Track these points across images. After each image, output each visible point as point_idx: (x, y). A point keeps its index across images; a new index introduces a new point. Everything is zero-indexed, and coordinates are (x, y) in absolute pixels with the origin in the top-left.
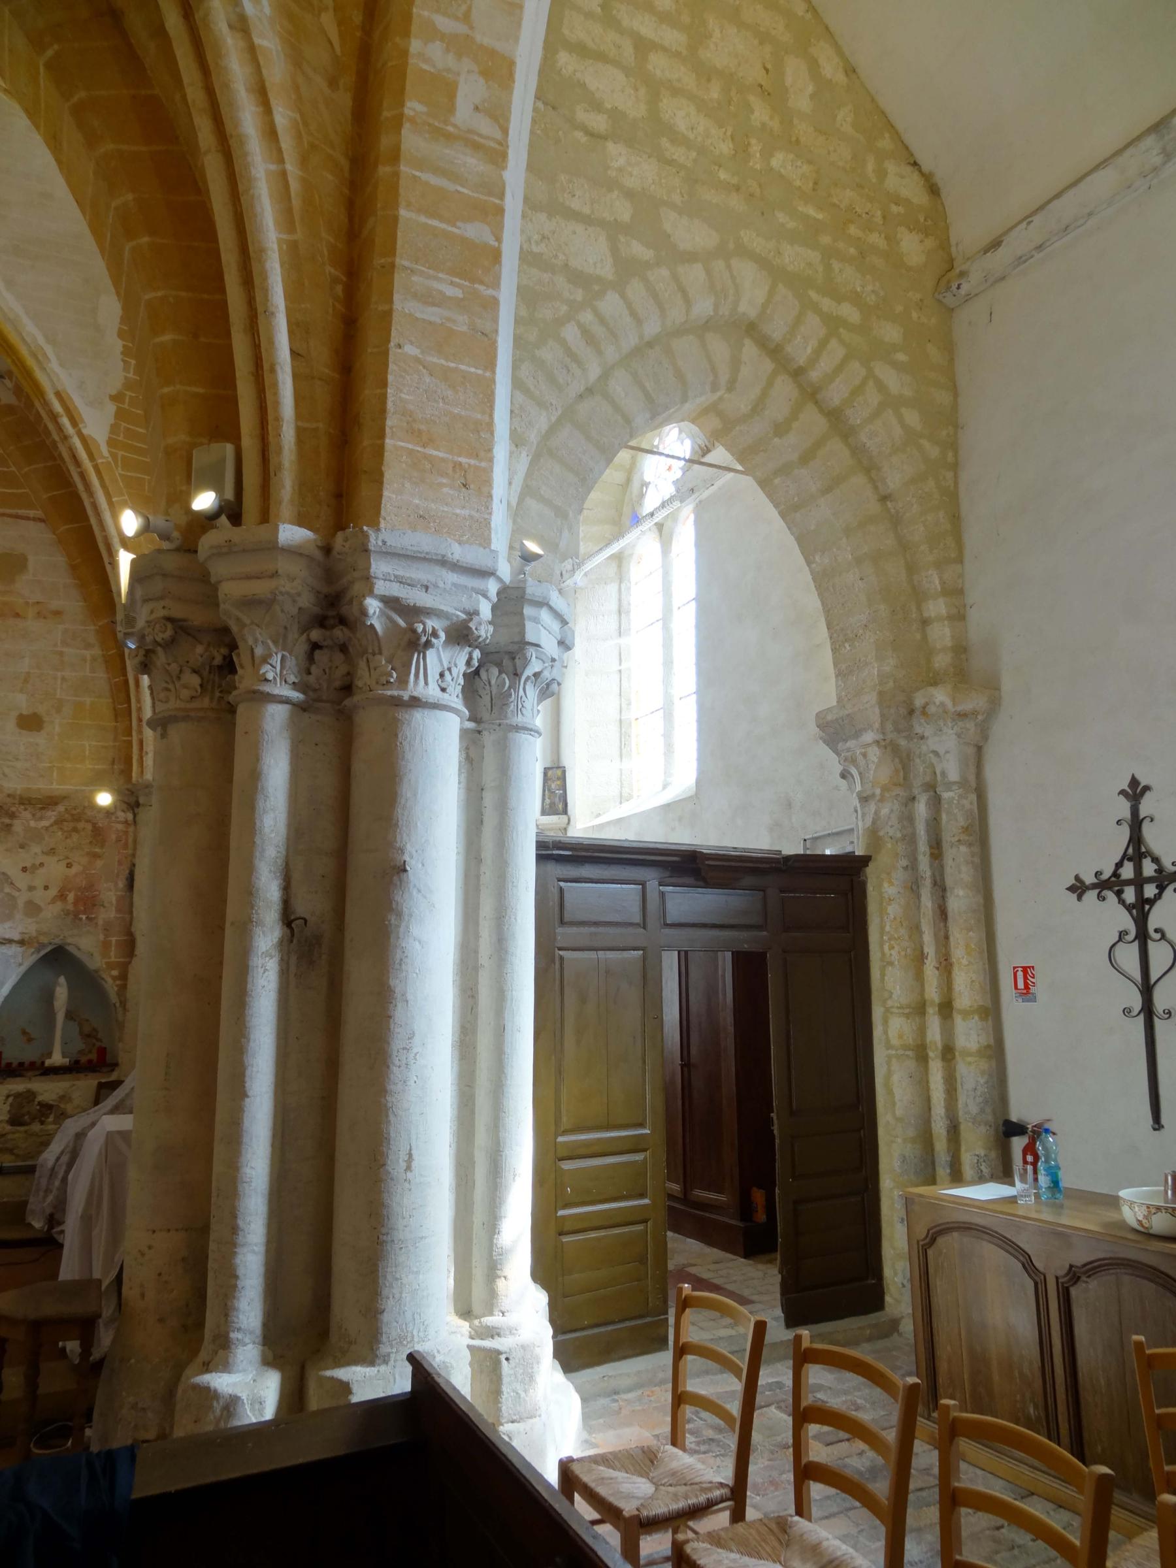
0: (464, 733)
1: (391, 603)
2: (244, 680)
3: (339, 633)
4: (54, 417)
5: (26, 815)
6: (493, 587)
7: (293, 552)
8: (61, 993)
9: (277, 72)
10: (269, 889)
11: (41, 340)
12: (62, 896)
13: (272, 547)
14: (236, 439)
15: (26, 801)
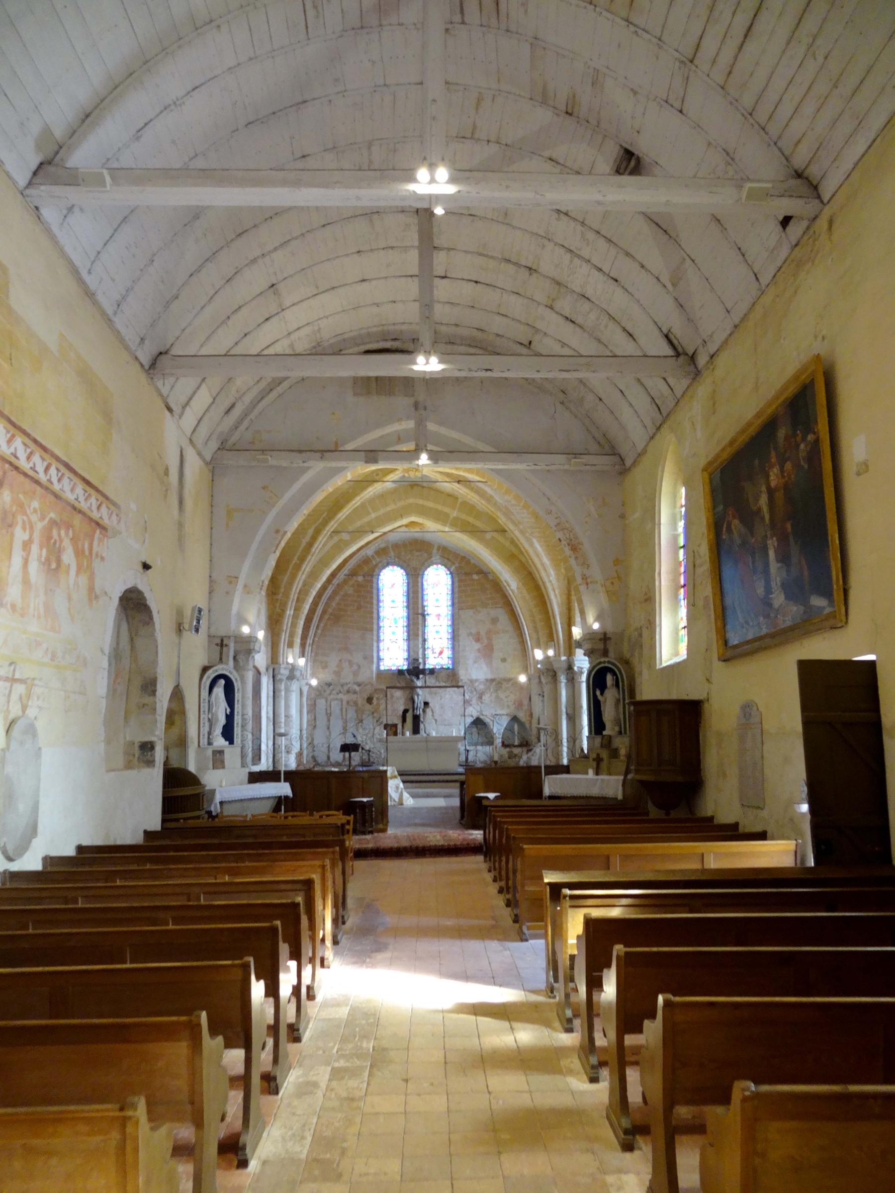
1: (578, 667)
4: (505, 587)
7: (564, 661)
8: (516, 727)
9: (556, 586)
10: (564, 710)
12: (515, 703)
14: (553, 641)
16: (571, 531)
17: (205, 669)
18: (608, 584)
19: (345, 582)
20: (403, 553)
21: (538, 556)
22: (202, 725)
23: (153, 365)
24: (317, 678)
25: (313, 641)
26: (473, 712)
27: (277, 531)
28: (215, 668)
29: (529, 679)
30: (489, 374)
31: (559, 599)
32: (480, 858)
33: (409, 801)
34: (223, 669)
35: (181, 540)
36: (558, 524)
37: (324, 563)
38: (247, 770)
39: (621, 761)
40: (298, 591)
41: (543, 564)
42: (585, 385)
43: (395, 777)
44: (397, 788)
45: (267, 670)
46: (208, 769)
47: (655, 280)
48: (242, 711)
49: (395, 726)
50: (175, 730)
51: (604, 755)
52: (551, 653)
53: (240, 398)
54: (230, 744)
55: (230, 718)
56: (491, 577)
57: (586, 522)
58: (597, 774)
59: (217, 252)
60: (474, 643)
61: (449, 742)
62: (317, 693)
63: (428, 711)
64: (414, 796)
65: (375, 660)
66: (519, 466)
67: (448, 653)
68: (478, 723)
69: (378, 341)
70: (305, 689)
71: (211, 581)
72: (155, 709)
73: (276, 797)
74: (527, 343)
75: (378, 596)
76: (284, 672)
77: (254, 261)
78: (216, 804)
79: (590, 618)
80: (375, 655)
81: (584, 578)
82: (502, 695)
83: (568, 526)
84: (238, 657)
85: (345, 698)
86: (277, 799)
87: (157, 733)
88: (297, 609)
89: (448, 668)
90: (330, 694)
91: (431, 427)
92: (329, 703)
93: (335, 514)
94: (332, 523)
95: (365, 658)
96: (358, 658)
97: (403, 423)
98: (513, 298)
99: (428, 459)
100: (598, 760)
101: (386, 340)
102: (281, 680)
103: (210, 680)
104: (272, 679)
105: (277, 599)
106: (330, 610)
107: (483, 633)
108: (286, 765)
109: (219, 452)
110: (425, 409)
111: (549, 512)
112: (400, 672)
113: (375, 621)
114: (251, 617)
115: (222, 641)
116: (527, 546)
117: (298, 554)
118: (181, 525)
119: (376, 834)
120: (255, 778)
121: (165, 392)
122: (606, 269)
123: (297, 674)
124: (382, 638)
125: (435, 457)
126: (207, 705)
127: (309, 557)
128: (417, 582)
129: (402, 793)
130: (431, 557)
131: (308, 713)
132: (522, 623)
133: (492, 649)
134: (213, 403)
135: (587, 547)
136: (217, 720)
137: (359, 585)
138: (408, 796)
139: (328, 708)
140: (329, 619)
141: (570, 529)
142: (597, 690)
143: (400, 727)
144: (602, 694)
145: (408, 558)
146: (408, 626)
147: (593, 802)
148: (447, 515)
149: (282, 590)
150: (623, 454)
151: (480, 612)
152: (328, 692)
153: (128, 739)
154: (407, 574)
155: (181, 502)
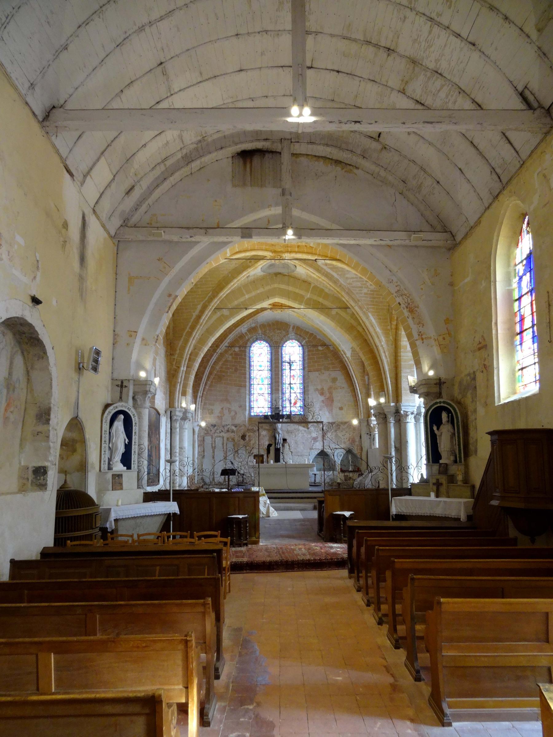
0: (415, 424)
1: (404, 411)
2: (388, 420)
3: (399, 414)
4: (342, 355)
5: (342, 426)
6: (416, 407)
7: (392, 406)
10: (393, 444)
11: (339, 342)
12: (349, 440)
13: (390, 406)
15: (342, 423)
16: (408, 297)
17: (107, 406)
18: (441, 338)
19: (226, 351)
20: (268, 331)
21: (372, 326)
22: (103, 453)
23: (47, 117)
24: (206, 422)
25: (203, 394)
26: (318, 446)
27: (170, 295)
28: (114, 405)
29: (360, 422)
30: (357, 127)
31: (388, 359)
32: (344, 573)
33: (274, 514)
34: (122, 406)
35: (82, 292)
36: (398, 291)
37: (210, 332)
38: (142, 491)
39: (459, 486)
40: (190, 352)
41: (376, 333)
42: (425, 171)
43: (264, 495)
44: (265, 503)
45: (166, 412)
46: (108, 490)
47: (518, 30)
48: (139, 442)
49: (262, 456)
50: (76, 459)
51: (443, 479)
52: (382, 400)
53: (139, 181)
54: (127, 469)
55: (128, 447)
56: (331, 348)
57: (422, 289)
58: (437, 496)
59: (104, 5)
60: (319, 396)
61: (304, 468)
62: (206, 432)
63: (286, 445)
64: (277, 509)
65: (247, 408)
66: (367, 241)
67: (300, 403)
68: (323, 454)
69: (252, 141)
70: (197, 429)
71: (115, 335)
72: (48, 437)
73: (165, 514)
74: (376, 136)
75: (250, 362)
76: (179, 414)
77: (142, 29)
78: (111, 522)
79: (425, 367)
80: (247, 404)
81: (420, 334)
82: (340, 434)
83: (406, 292)
84: (136, 397)
85: (226, 435)
86: (166, 517)
87: (51, 458)
88: (189, 367)
89: (301, 414)
90: (214, 433)
91: (296, 212)
92: (214, 440)
93: (218, 293)
94: (216, 300)
95: (240, 407)
96: (235, 406)
97: (272, 209)
98: (370, 84)
99: (293, 235)
100: (438, 485)
101: (258, 140)
102: (176, 420)
103: (111, 414)
104: (169, 420)
105: (174, 359)
106: (215, 372)
107: (326, 388)
108: (180, 486)
109: (122, 228)
110: (291, 194)
111: (391, 282)
112: (266, 417)
113: (247, 380)
114: (148, 365)
115: (122, 382)
116: (364, 319)
117: (190, 324)
118: (81, 279)
119: (250, 546)
120: (149, 497)
121: (64, 152)
122: (464, 34)
123: (189, 415)
124: (252, 392)
125: (299, 233)
126: (108, 435)
127: (198, 327)
128: (278, 352)
129: (268, 507)
130: (289, 334)
131: (199, 446)
132: (354, 381)
133: (332, 401)
134: (114, 179)
135: (423, 310)
136: (116, 449)
137: (236, 354)
138: (274, 510)
139: (214, 443)
140: (214, 378)
141: (408, 295)
142: (434, 425)
143: (265, 457)
144: (438, 429)
145: (271, 334)
146: (271, 384)
147: (447, 524)
148: (302, 297)
149: (178, 352)
150: (454, 230)
151: (323, 373)
152: (213, 431)
153: (23, 464)
154: (270, 346)
155: (82, 259)
